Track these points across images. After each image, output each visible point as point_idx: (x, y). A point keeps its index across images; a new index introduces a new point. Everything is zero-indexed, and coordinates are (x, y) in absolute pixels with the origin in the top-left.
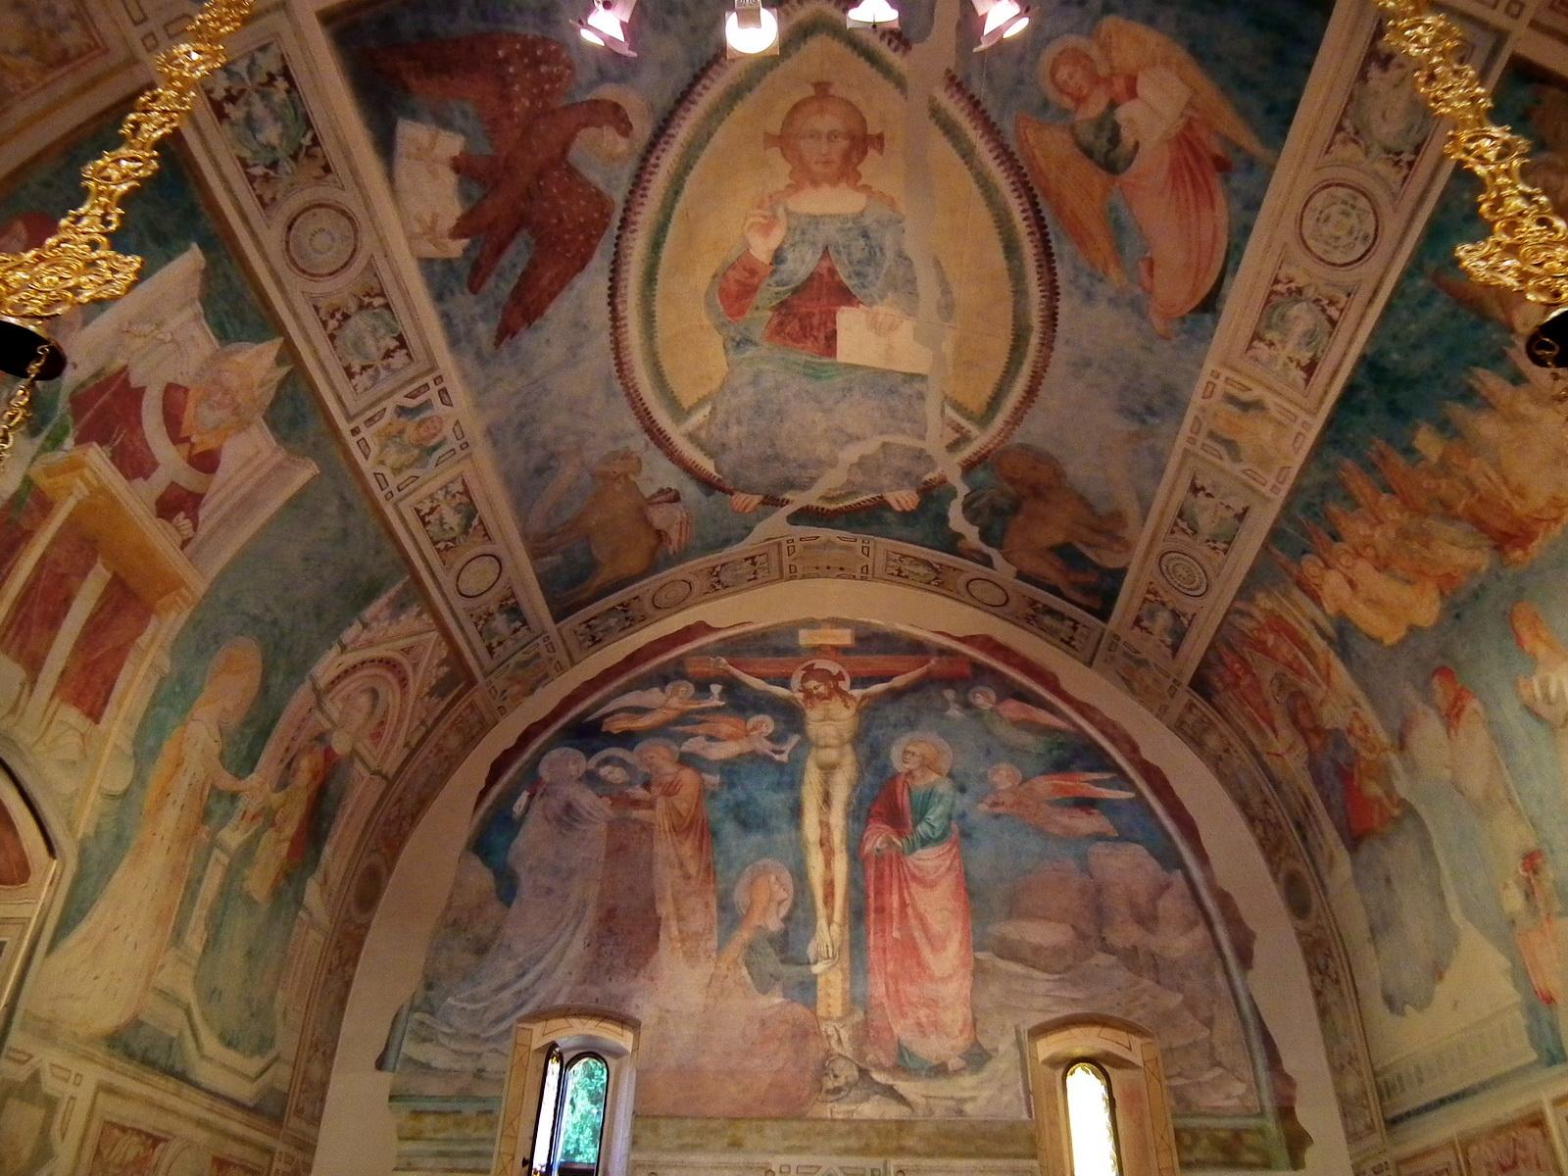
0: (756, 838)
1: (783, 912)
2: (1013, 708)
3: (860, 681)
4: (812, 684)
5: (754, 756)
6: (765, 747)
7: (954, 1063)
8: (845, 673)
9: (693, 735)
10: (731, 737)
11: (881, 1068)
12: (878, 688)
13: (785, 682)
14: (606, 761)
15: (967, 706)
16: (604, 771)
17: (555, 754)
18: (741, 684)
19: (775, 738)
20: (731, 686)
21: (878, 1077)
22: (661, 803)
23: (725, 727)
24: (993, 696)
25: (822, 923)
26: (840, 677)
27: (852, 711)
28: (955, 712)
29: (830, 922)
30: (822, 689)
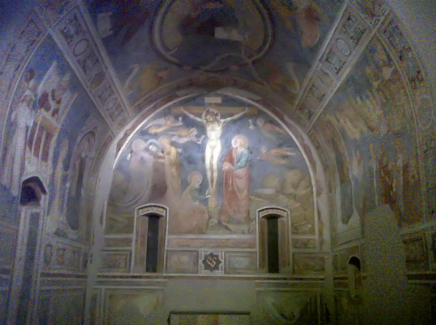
0: (192, 166)
1: (200, 183)
2: (269, 126)
3: (223, 117)
4: (208, 117)
5: (192, 142)
6: (194, 139)
7: (242, 220)
8: (219, 114)
9: (174, 136)
10: (185, 136)
11: (224, 221)
12: (229, 119)
13: (200, 117)
14: (151, 144)
15: (255, 125)
16: (151, 147)
17: (136, 141)
18: (188, 117)
19: (198, 136)
20: (185, 118)
21: (224, 223)
22: (166, 156)
23: (184, 132)
24: (263, 122)
25: (210, 186)
26: (217, 115)
27: (221, 126)
28: (251, 127)
29: (212, 186)
30: (211, 119)
